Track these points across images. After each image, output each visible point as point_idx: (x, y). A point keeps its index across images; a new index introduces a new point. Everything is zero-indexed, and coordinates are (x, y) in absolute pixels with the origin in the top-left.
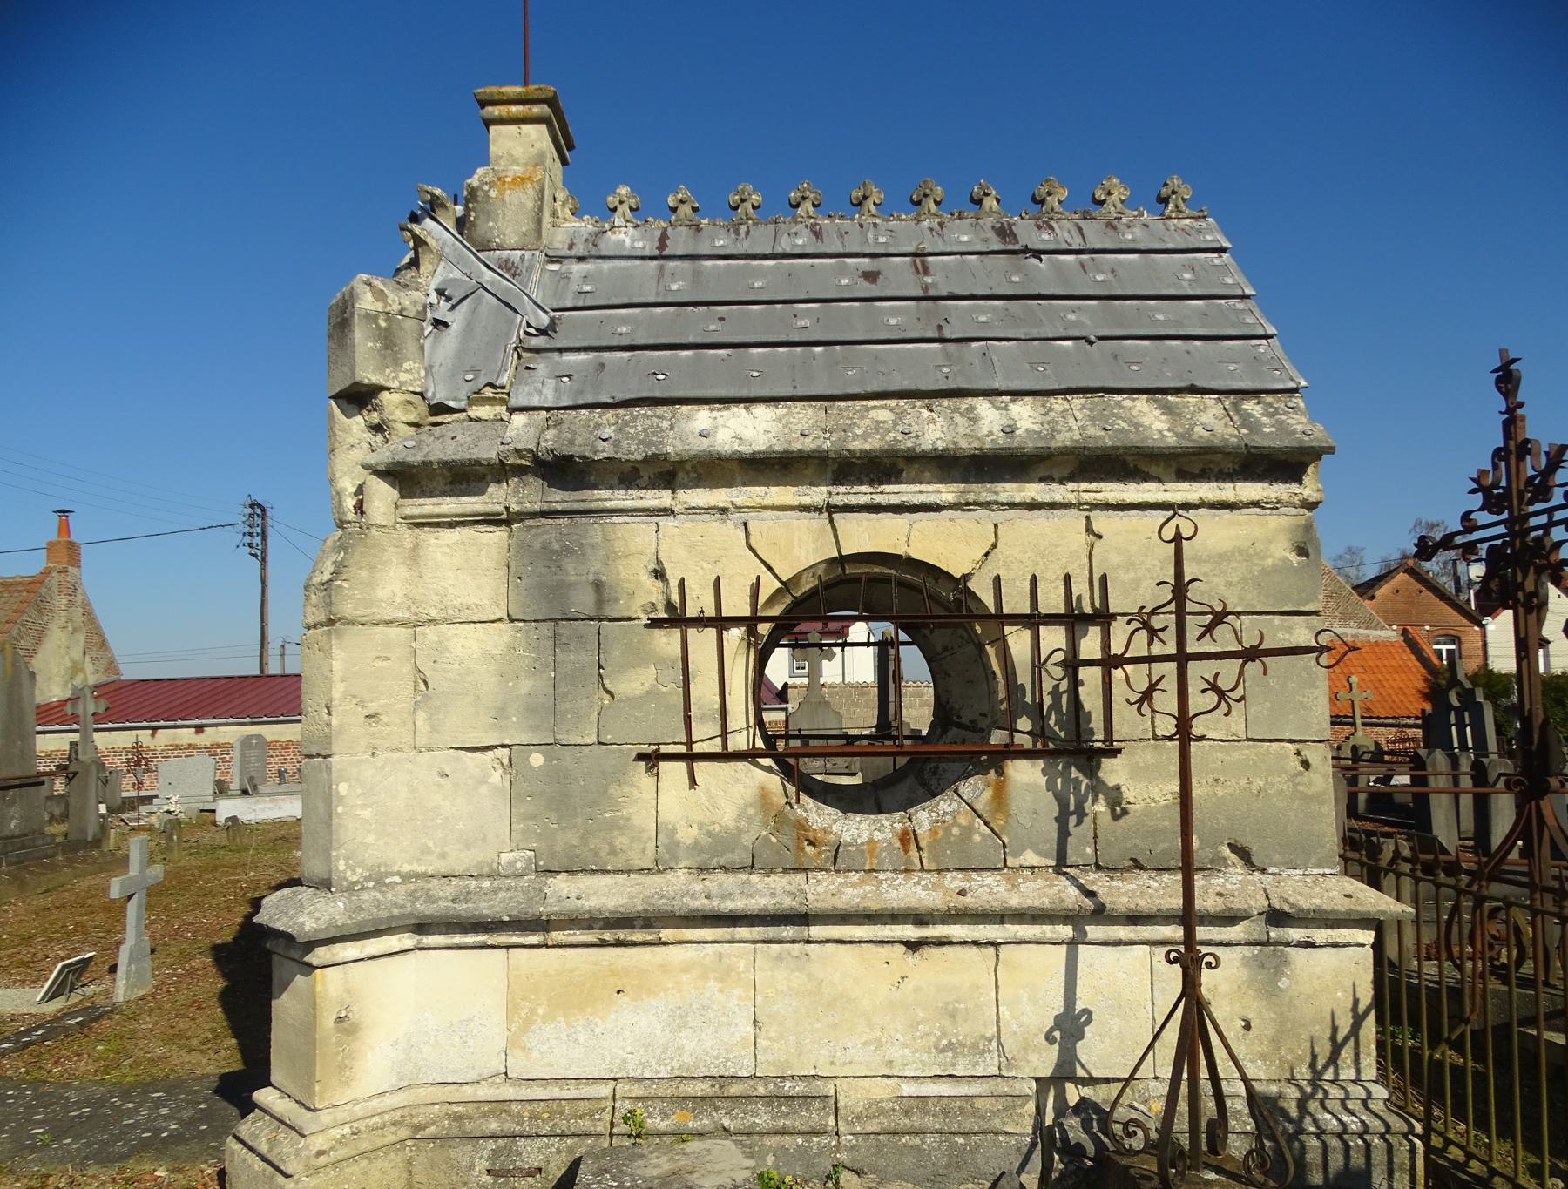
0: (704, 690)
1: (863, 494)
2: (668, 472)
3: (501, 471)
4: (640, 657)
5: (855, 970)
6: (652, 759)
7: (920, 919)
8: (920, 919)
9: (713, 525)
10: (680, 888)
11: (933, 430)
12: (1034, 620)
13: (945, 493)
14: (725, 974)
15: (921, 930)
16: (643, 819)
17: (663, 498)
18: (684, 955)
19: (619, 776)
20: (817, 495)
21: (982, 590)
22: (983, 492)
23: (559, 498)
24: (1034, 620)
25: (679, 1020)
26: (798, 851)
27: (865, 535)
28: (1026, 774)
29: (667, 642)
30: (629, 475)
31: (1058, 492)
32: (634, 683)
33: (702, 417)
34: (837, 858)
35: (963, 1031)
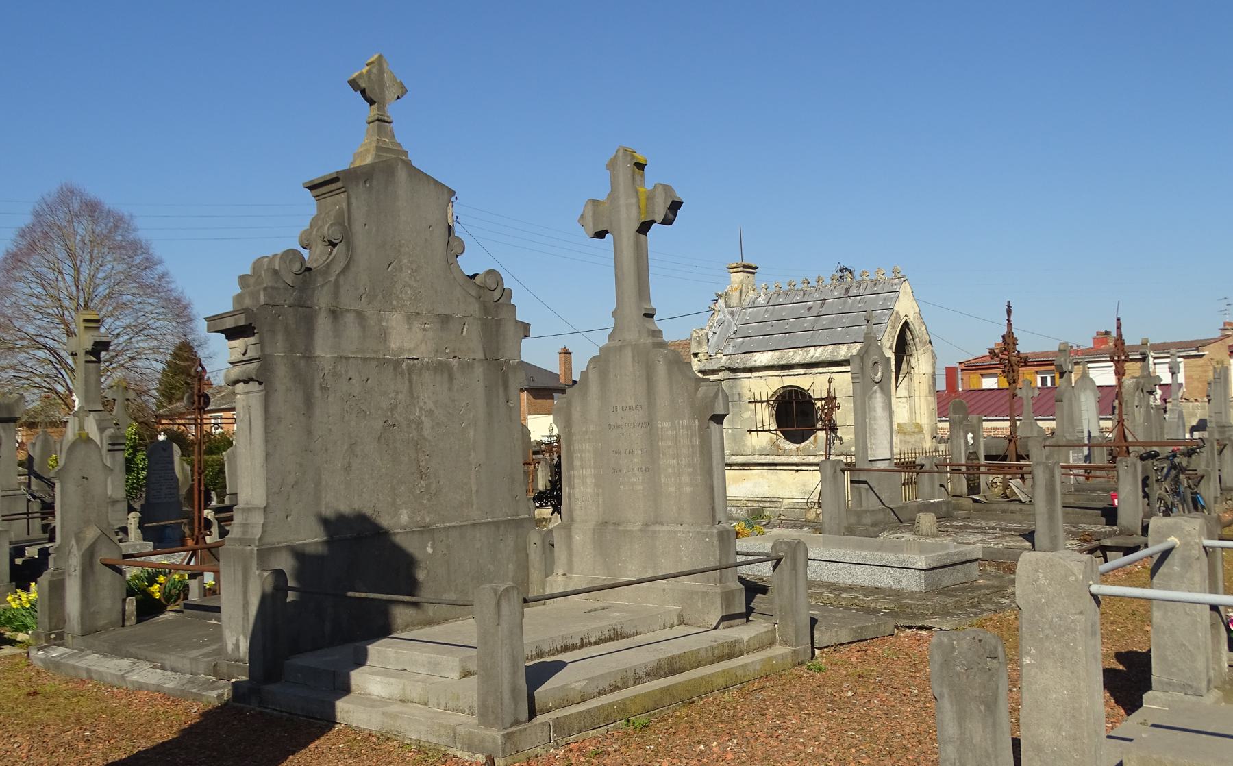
0: (759, 417)
1: (787, 372)
2: (751, 370)
3: (720, 370)
4: (748, 409)
5: (786, 475)
6: (750, 431)
7: (797, 465)
8: (797, 465)
9: (762, 381)
10: (756, 459)
11: (798, 357)
12: (821, 399)
13: (802, 371)
14: (763, 476)
15: (798, 466)
16: (749, 444)
17: (749, 375)
18: (755, 472)
19: (744, 435)
20: (778, 373)
21: (811, 392)
22: (809, 370)
23: (732, 375)
24: (821, 399)
25: (755, 486)
26: (778, 450)
27: (789, 381)
28: (821, 435)
29: (752, 406)
30: (745, 370)
31: (825, 370)
32: (747, 415)
33: (758, 355)
34: (785, 453)
35: (806, 489)
